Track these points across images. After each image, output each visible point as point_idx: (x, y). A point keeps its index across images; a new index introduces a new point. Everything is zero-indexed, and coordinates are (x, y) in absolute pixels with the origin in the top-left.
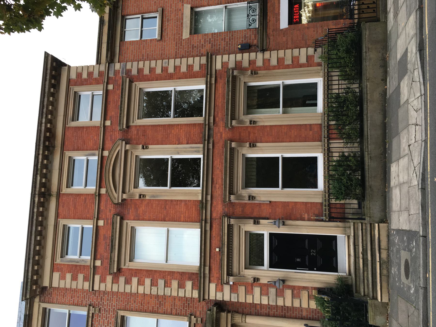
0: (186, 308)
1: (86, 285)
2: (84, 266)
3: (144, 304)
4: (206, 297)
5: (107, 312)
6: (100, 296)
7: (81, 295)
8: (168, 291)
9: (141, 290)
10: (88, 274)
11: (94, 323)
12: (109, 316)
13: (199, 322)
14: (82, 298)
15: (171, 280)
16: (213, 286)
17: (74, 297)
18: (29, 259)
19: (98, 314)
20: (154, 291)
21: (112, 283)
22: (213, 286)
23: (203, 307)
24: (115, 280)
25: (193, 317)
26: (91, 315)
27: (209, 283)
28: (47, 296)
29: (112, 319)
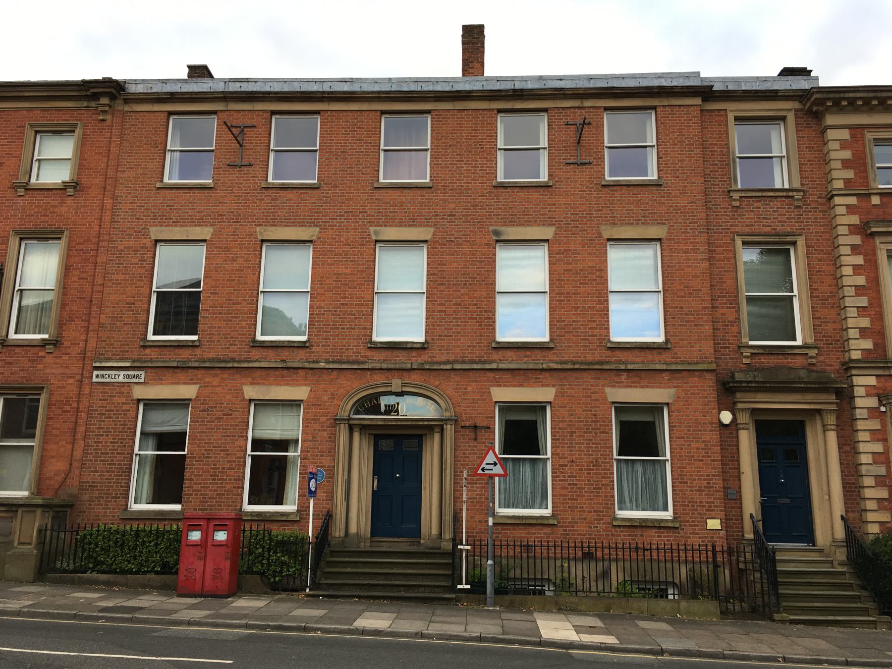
0: (826, 340)
1: (839, 184)
2: (867, 178)
3: (820, 275)
4: (854, 372)
5: (798, 218)
6: (819, 205)
7: (816, 174)
8: (852, 312)
9: (847, 271)
10: (856, 184)
11: (779, 199)
12: (791, 222)
13: (810, 360)
14: (811, 178)
15: (869, 316)
16: (872, 381)
17: (810, 164)
18: (874, 91)
19: (792, 205)
20: (848, 291)
21: (849, 225)
22: (872, 381)
23: (831, 366)
24: (854, 230)
25: (816, 351)
26: (791, 194)
27: (877, 376)
28: (805, 121)
29: (789, 228)
